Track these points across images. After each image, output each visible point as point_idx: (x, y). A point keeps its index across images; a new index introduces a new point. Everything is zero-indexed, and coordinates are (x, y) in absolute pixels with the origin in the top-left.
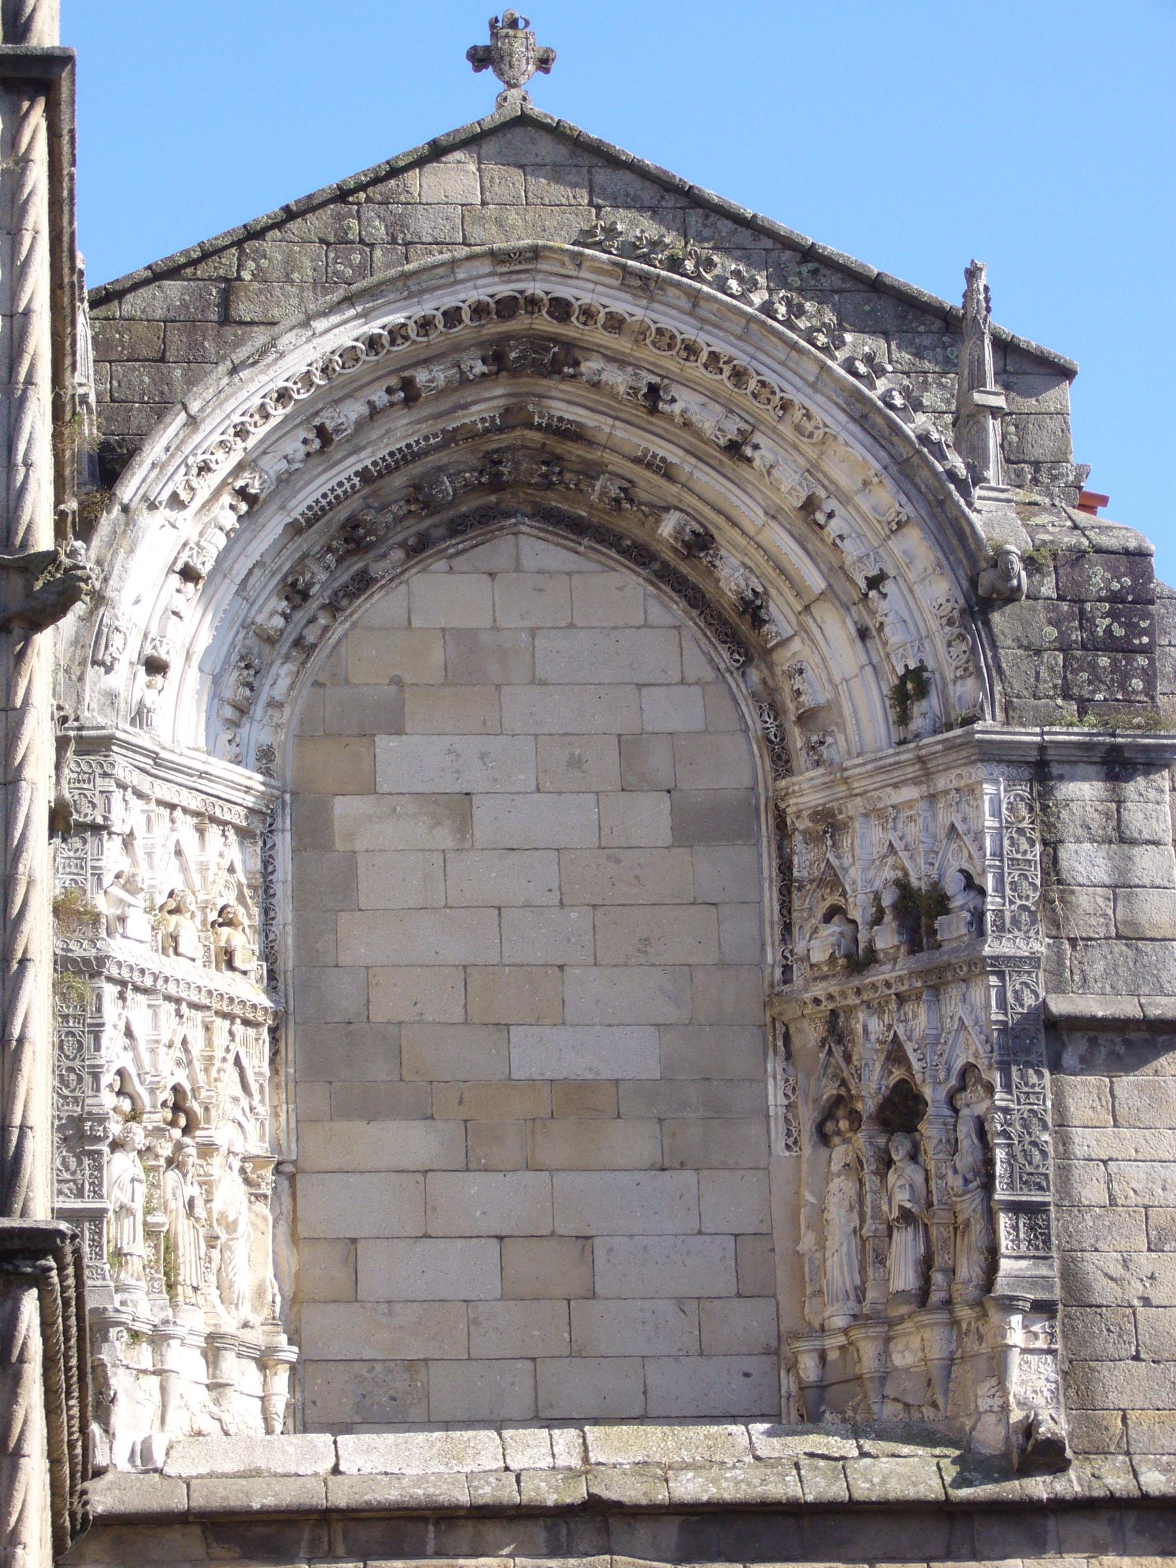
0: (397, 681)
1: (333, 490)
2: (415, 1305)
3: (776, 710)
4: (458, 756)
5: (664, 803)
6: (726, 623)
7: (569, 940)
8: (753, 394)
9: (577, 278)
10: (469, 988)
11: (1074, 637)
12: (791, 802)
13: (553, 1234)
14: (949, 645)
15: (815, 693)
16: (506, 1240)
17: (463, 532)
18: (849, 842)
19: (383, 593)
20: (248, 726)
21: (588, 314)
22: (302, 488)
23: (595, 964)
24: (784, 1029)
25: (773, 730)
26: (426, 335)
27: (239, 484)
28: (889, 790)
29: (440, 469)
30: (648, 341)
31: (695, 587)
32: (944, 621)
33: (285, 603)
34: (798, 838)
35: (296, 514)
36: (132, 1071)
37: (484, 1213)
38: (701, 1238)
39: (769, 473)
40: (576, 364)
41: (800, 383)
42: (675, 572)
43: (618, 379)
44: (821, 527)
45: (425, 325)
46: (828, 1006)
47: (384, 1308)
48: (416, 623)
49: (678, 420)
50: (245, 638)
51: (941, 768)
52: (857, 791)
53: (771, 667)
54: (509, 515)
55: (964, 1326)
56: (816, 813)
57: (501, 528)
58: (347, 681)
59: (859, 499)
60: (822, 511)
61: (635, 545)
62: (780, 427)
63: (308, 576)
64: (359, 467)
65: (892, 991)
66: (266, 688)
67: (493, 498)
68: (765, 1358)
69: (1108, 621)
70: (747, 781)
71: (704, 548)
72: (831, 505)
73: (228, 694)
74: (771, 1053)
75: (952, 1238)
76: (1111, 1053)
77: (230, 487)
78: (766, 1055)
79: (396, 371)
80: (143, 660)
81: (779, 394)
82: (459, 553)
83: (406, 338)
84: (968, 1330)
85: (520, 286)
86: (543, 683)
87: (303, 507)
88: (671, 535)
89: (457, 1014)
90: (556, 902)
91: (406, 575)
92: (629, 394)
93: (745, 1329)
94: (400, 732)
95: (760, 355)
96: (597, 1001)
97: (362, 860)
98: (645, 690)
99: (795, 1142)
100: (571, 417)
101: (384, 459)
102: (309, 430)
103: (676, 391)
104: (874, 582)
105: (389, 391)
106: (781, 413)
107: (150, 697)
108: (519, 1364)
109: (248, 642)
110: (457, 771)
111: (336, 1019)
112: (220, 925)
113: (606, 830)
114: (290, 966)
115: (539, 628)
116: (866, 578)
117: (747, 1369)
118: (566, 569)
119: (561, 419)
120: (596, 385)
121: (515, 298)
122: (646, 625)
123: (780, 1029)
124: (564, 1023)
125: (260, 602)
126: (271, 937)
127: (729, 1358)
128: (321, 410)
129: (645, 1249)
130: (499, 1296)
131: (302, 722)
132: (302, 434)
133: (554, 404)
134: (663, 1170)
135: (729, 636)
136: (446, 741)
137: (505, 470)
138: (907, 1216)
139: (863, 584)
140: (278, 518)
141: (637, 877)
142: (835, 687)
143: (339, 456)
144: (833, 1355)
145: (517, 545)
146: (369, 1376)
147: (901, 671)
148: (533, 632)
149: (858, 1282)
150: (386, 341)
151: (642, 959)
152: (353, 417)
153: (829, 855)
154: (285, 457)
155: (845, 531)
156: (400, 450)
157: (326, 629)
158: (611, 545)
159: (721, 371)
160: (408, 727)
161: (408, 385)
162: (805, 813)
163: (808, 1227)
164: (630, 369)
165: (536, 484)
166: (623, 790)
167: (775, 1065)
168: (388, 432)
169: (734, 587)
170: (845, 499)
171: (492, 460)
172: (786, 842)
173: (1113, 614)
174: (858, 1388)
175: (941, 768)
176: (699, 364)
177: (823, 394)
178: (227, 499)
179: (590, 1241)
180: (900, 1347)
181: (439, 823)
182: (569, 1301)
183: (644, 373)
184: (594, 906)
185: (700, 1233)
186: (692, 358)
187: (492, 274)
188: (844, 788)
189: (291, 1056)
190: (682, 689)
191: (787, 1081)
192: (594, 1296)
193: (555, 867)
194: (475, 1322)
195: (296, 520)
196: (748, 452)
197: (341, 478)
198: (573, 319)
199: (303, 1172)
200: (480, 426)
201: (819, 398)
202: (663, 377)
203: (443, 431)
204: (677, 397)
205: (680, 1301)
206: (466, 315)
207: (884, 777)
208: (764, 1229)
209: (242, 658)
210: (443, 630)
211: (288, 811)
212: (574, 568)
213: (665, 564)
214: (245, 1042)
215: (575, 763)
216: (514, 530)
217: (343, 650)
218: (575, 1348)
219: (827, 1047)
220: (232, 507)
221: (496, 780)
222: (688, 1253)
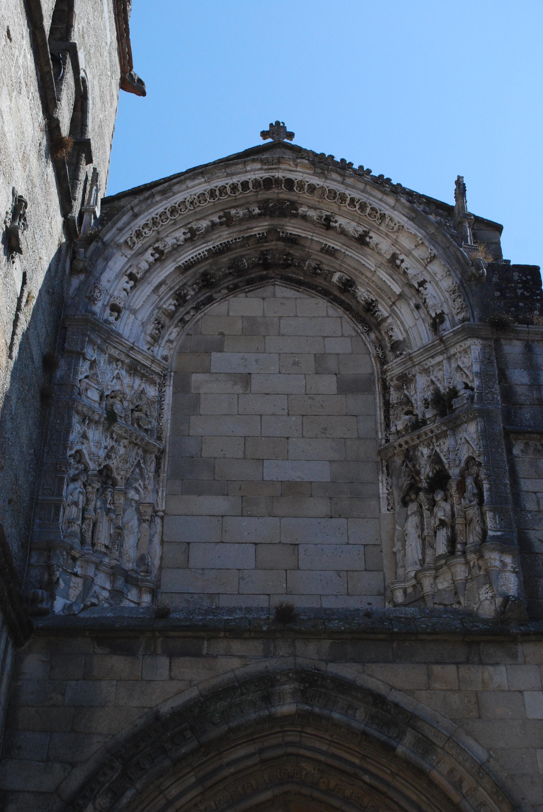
0: (222, 334)
1: (196, 256)
2: (214, 570)
3: (382, 347)
4: (246, 360)
5: (334, 378)
6: (361, 316)
7: (291, 428)
8: (368, 214)
9: (296, 171)
10: (246, 445)
11: (508, 295)
12: (388, 374)
13: (280, 543)
14: (454, 301)
15: (398, 335)
16: (259, 545)
17: (252, 284)
18: (413, 385)
19: (218, 303)
20: (157, 347)
21: (301, 185)
22: (183, 254)
23: (302, 437)
24: (386, 464)
25: (381, 354)
26: (234, 193)
27: (156, 245)
28: (430, 360)
29: (242, 256)
30: (325, 196)
31: (348, 304)
32: (452, 292)
33: (175, 302)
34: (392, 389)
35: (180, 263)
36: (85, 451)
37: (249, 533)
38: (349, 546)
39: (377, 247)
40: (297, 210)
41: (388, 207)
42: (339, 298)
43: (313, 214)
44: (398, 267)
45: (234, 188)
46: (406, 447)
47: (200, 571)
48: (231, 314)
49: (339, 230)
50: (158, 313)
51: (452, 344)
52: (416, 363)
53: (380, 332)
54: (271, 278)
55: (472, 564)
56: (399, 377)
57: (268, 283)
58: (201, 334)
59: (413, 252)
60: (398, 259)
61: (323, 289)
62: (381, 228)
63: (185, 291)
64: (207, 248)
65: (434, 434)
66: (167, 335)
67: (265, 272)
68: (378, 597)
69: (522, 290)
70: (369, 371)
71: (351, 286)
72: (402, 257)
73: (149, 332)
74: (381, 473)
75: (465, 530)
76: (535, 449)
77: (152, 248)
78: (378, 474)
79: (223, 210)
80: (110, 304)
81: (379, 212)
82: (250, 291)
83: (226, 194)
84: (474, 566)
85: (273, 174)
86: (284, 335)
87: (183, 261)
88: (337, 281)
89: (241, 455)
90: (286, 413)
91: (228, 298)
92: (318, 219)
93: (369, 584)
94: (221, 351)
95: (371, 198)
96: (303, 451)
97: (202, 397)
98: (326, 339)
99: (392, 508)
100: (295, 233)
101: (217, 246)
102: (186, 229)
103: (337, 218)
104: (422, 284)
105: (220, 218)
106: (380, 221)
107: (112, 319)
108: (262, 597)
109: (159, 315)
110: (245, 366)
111: (187, 455)
112: (136, 411)
113: (308, 388)
114: (168, 435)
115: (282, 317)
116: (418, 283)
117: (370, 601)
118: (294, 297)
119: (291, 234)
120: (304, 217)
121: (270, 178)
122: (327, 316)
123: (384, 463)
124: (288, 460)
125: (165, 299)
126: (161, 424)
127: (361, 597)
128: (192, 222)
129: (322, 550)
130: (253, 568)
131: (181, 347)
132: (183, 230)
133: (288, 228)
134: (331, 517)
135: (362, 321)
136: (241, 355)
137: (269, 258)
138: (442, 523)
139: (416, 286)
140: (173, 264)
141: (321, 405)
142: (407, 332)
143: (199, 243)
144: (410, 590)
145: (274, 289)
146: (191, 600)
147: (434, 315)
148: (280, 318)
149: (421, 557)
150: (217, 193)
151: (323, 436)
152: (205, 225)
153: (405, 392)
154: (176, 238)
155: (409, 266)
156: (225, 243)
157: (194, 315)
158: (313, 289)
159: (355, 206)
160: (225, 350)
161: (227, 215)
162: (394, 379)
163: (398, 540)
164: (318, 210)
165: (282, 264)
166: (316, 373)
167: (382, 477)
168: (219, 236)
169: (363, 299)
170: (409, 253)
171: (263, 254)
172: (387, 395)
173: (524, 288)
174: (422, 603)
175: (452, 344)
176: (346, 204)
177: (397, 211)
178: (150, 251)
179: (297, 546)
180: (441, 580)
181: (236, 384)
182: (286, 570)
183: (324, 211)
184: (303, 416)
185: (348, 544)
186: (343, 202)
187: (261, 169)
188: (410, 362)
189: (166, 469)
190: (342, 338)
191: (388, 483)
192: (298, 568)
193: (286, 401)
194: (243, 578)
195: (180, 266)
196: (368, 239)
197: (200, 252)
198: (295, 189)
199: (167, 515)
200: (258, 236)
201: (396, 212)
202: (332, 213)
203: (243, 237)
204: (338, 220)
205: (338, 572)
206: (251, 186)
207: (428, 354)
208: (377, 543)
209: (156, 320)
210: (242, 317)
211: (172, 378)
212: (298, 297)
213: (335, 296)
214: (144, 458)
215: (296, 364)
216: (273, 283)
217: (200, 323)
218: (288, 590)
219: (405, 463)
220: (152, 255)
221: (262, 369)
222: (342, 552)
